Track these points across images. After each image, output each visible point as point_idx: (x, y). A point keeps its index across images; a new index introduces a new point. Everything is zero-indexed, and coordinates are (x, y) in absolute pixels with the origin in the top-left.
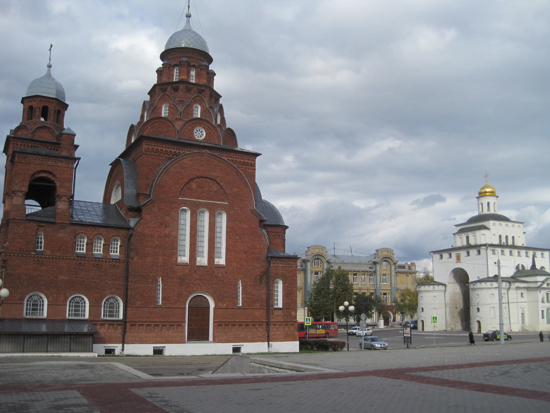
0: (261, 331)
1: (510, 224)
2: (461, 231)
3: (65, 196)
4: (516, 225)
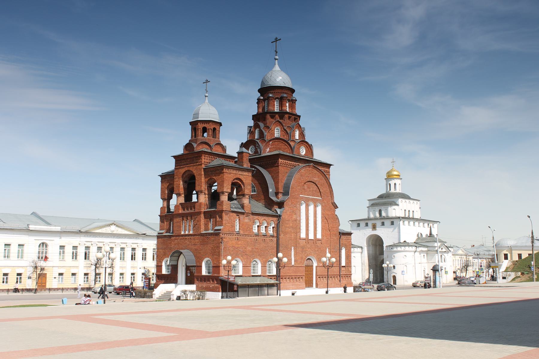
0: (302, 282)
1: (412, 201)
2: (373, 205)
3: (247, 195)
4: (415, 202)
